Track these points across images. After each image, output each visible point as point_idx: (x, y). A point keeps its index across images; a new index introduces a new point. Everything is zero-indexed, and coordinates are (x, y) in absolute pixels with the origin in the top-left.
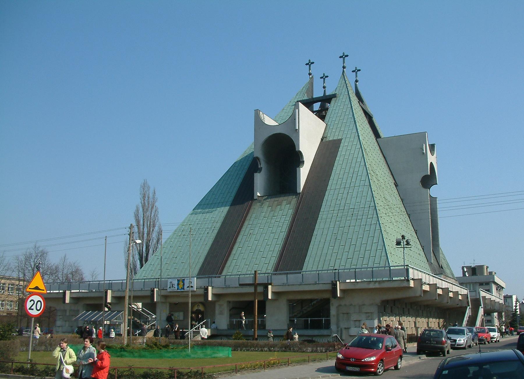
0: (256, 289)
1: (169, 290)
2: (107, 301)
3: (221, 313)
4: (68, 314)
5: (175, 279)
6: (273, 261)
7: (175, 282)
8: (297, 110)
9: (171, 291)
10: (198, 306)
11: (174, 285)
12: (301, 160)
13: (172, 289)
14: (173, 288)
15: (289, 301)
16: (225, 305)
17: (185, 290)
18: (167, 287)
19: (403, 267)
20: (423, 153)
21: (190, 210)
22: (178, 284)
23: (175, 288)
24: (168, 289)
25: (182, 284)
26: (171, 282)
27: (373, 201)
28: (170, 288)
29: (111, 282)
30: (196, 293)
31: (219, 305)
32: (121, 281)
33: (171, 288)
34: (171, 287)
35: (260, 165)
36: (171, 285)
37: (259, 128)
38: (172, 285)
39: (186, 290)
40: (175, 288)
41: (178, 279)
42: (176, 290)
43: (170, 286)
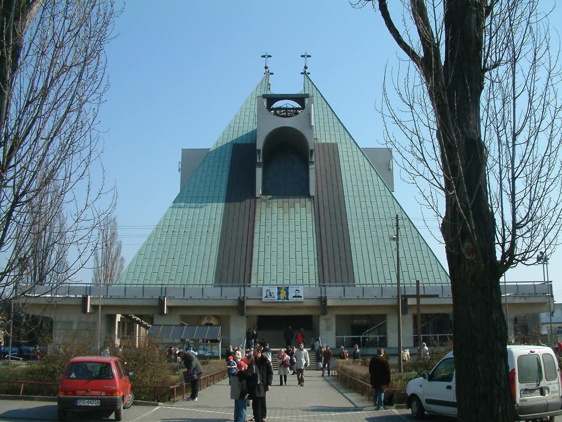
0: (418, 301)
1: (264, 300)
2: (87, 311)
3: (328, 329)
4: (75, 327)
5: (275, 286)
6: (313, 270)
7: (275, 291)
8: (313, 105)
9: (268, 301)
10: (209, 319)
11: (272, 294)
12: (310, 160)
13: (270, 298)
14: (272, 298)
15: (338, 317)
16: (334, 319)
17: (290, 301)
18: (261, 295)
19: (378, 286)
20: (390, 169)
21: (171, 203)
22: (279, 293)
23: (274, 297)
24: (263, 298)
25: (285, 292)
26: (268, 290)
27: (403, 213)
28: (267, 297)
29: (89, 285)
30: (304, 304)
31: (325, 319)
32: (85, 285)
33: (268, 297)
34: (268, 296)
35: (259, 159)
36: (268, 294)
37: (264, 118)
38: (270, 293)
39: (291, 301)
40: (274, 297)
41: (278, 286)
42: (275, 301)
43: (267, 295)
